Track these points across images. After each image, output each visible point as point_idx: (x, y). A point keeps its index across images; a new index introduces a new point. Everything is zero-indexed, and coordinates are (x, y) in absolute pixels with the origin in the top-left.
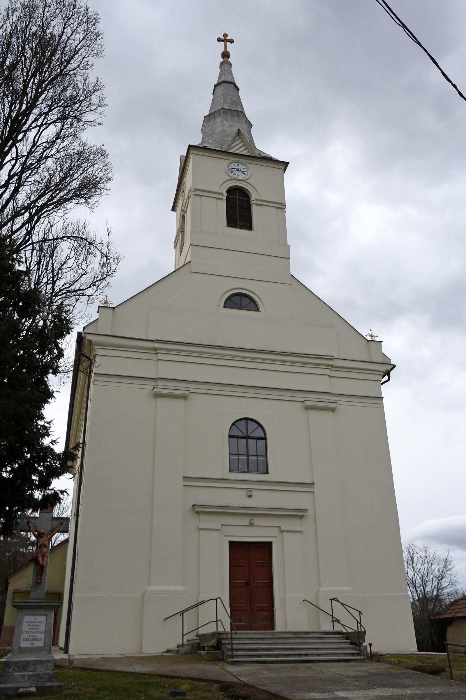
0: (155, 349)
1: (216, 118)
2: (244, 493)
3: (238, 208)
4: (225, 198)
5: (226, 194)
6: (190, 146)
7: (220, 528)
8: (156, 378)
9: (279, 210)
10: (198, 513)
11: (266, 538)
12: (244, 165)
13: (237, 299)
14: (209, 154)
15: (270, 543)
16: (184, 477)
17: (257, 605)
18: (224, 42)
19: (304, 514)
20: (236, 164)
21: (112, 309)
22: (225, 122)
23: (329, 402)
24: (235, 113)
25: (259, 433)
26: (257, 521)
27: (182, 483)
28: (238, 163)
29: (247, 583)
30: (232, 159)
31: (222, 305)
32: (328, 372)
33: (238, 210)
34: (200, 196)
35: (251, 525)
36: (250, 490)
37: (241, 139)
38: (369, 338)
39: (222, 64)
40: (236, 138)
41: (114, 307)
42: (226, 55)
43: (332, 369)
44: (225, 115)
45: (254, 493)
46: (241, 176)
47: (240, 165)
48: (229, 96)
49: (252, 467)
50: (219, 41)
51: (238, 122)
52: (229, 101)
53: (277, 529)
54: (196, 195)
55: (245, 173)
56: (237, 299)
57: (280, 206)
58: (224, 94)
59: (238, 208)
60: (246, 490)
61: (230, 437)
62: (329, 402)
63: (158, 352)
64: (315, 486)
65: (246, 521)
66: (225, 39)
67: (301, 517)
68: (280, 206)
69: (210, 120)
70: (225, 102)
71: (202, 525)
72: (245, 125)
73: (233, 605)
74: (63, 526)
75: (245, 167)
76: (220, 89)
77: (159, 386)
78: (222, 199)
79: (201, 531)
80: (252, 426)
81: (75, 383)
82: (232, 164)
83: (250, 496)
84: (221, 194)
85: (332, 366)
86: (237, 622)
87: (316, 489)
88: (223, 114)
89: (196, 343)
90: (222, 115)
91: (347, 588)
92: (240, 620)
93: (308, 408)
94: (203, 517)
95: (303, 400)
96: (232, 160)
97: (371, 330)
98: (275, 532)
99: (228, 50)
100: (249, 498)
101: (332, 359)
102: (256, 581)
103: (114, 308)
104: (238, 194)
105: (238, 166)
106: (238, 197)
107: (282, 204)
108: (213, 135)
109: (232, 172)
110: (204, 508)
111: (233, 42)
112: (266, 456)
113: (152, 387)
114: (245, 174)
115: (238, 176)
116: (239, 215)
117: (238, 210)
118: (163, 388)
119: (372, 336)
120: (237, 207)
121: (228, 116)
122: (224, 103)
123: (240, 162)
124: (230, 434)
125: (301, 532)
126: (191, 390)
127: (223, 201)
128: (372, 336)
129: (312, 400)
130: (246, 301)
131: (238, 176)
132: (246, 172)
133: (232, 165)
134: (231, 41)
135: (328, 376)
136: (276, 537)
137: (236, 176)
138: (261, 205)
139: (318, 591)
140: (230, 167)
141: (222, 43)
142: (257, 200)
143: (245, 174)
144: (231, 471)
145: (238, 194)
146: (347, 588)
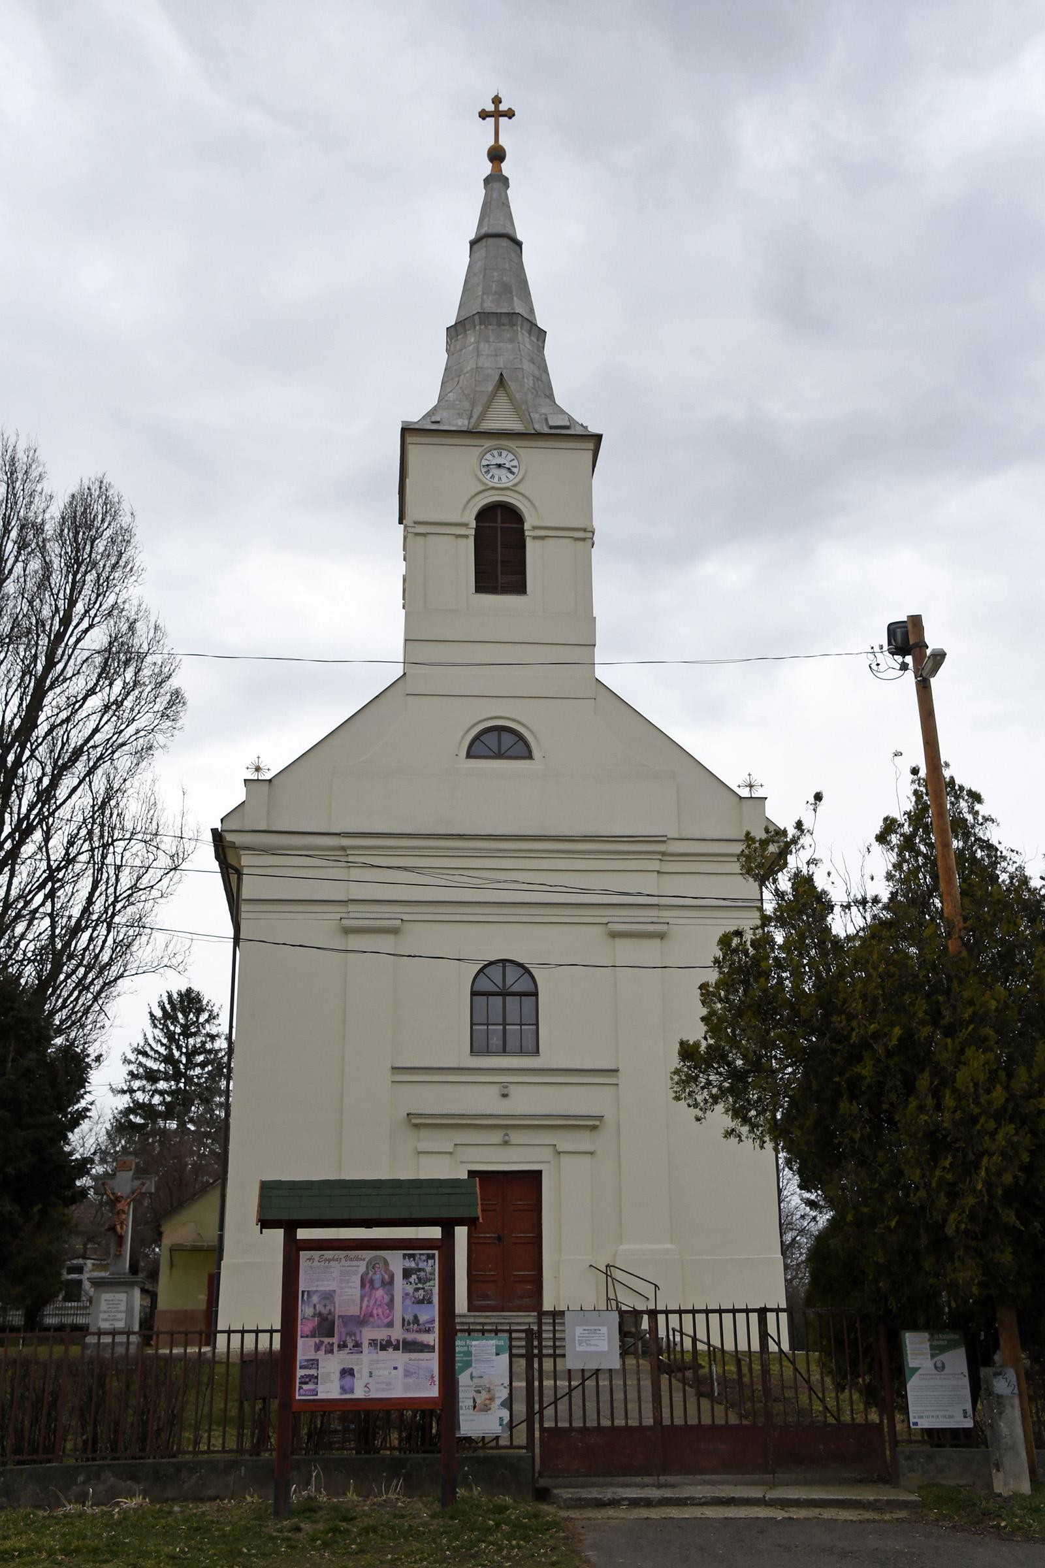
0: (343, 848)
1: (468, 332)
2: (495, 1089)
3: (499, 547)
4: (473, 532)
5: (473, 524)
6: (405, 431)
7: (451, 1150)
8: (347, 899)
9: (580, 544)
10: (416, 1126)
11: (531, 1164)
12: (512, 453)
13: (491, 740)
14: (443, 439)
15: (540, 1172)
16: (393, 1068)
17: (515, 1273)
18: (493, 119)
19: (597, 1123)
20: (495, 453)
21: (267, 782)
22: (482, 345)
23: (652, 923)
24: (504, 320)
25: (523, 985)
26: (516, 1137)
27: (388, 1077)
28: (500, 449)
29: (499, 1239)
30: (488, 443)
31: (464, 754)
32: (656, 865)
33: (499, 552)
34: (424, 535)
35: (506, 1143)
36: (505, 1085)
37: (508, 396)
38: (744, 792)
39: (487, 181)
40: (496, 393)
41: (269, 778)
42: (497, 155)
43: (664, 858)
44: (483, 327)
45: (513, 1090)
46: (506, 479)
47: (504, 453)
48: (495, 274)
49: (512, 1042)
50: (484, 119)
51: (511, 340)
52: (494, 288)
53: (550, 1150)
54: (417, 534)
55: (514, 470)
56: (491, 740)
57: (581, 535)
58: (485, 269)
59: (499, 547)
60: (499, 1085)
61: (474, 994)
62: (652, 923)
63: (348, 853)
64: (620, 1074)
65: (496, 1137)
66: (497, 113)
67: (594, 1128)
68: (581, 535)
69: (458, 336)
70: (487, 291)
71: (423, 1146)
72: (527, 339)
73: (475, 1273)
74: (145, 1187)
75: (513, 457)
76: (481, 247)
77: (351, 915)
78: (466, 536)
79: (421, 1155)
80: (512, 973)
81: (229, 890)
82: (488, 454)
83: (505, 1096)
84: (466, 525)
85: (664, 854)
86: (481, 1300)
87: (622, 1079)
88: (481, 324)
89: (413, 833)
90: (477, 328)
91: (668, 1246)
92: (485, 1297)
93: (614, 935)
94: (424, 1133)
95: (605, 920)
96: (488, 445)
97: (749, 775)
98: (546, 1154)
99: (501, 143)
100: (503, 1098)
101: (664, 842)
102: (514, 1235)
103: (270, 781)
104: (499, 517)
105: (501, 455)
106: (499, 524)
107: (585, 530)
108: (459, 376)
109: (488, 472)
110: (425, 1118)
111: (514, 115)
112: (537, 1024)
113: (338, 916)
114: (513, 473)
115: (500, 479)
116: (502, 562)
117: (499, 552)
118: (360, 916)
119: (751, 786)
120: (497, 548)
121: (490, 327)
122: (483, 294)
123: (503, 447)
124: (474, 989)
125: (591, 1153)
126: (405, 917)
127: (469, 539)
128: (751, 786)
129: (622, 920)
130: (507, 740)
131: (500, 479)
132: (515, 467)
133: (488, 456)
134: (510, 114)
135: (656, 873)
136: (549, 1162)
137: (496, 479)
138: (543, 538)
139: (616, 1252)
140: (484, 463)
141: (491, 121)
142: (534, 528)
143: (513, 473)
144: (473, 1052)
145: (499, 517)
146: (668, 1246)
